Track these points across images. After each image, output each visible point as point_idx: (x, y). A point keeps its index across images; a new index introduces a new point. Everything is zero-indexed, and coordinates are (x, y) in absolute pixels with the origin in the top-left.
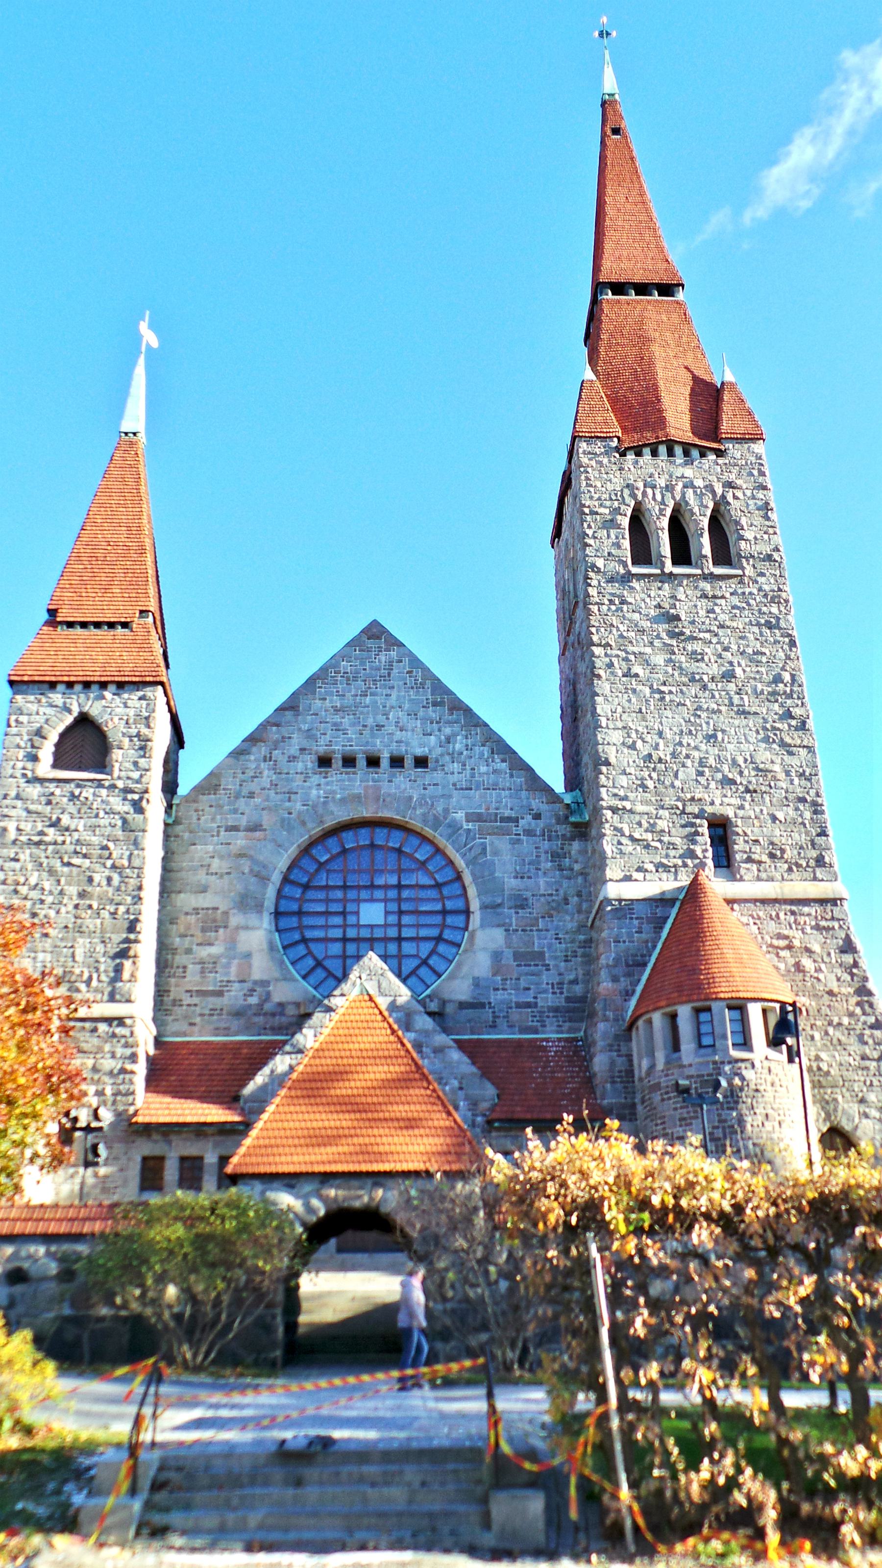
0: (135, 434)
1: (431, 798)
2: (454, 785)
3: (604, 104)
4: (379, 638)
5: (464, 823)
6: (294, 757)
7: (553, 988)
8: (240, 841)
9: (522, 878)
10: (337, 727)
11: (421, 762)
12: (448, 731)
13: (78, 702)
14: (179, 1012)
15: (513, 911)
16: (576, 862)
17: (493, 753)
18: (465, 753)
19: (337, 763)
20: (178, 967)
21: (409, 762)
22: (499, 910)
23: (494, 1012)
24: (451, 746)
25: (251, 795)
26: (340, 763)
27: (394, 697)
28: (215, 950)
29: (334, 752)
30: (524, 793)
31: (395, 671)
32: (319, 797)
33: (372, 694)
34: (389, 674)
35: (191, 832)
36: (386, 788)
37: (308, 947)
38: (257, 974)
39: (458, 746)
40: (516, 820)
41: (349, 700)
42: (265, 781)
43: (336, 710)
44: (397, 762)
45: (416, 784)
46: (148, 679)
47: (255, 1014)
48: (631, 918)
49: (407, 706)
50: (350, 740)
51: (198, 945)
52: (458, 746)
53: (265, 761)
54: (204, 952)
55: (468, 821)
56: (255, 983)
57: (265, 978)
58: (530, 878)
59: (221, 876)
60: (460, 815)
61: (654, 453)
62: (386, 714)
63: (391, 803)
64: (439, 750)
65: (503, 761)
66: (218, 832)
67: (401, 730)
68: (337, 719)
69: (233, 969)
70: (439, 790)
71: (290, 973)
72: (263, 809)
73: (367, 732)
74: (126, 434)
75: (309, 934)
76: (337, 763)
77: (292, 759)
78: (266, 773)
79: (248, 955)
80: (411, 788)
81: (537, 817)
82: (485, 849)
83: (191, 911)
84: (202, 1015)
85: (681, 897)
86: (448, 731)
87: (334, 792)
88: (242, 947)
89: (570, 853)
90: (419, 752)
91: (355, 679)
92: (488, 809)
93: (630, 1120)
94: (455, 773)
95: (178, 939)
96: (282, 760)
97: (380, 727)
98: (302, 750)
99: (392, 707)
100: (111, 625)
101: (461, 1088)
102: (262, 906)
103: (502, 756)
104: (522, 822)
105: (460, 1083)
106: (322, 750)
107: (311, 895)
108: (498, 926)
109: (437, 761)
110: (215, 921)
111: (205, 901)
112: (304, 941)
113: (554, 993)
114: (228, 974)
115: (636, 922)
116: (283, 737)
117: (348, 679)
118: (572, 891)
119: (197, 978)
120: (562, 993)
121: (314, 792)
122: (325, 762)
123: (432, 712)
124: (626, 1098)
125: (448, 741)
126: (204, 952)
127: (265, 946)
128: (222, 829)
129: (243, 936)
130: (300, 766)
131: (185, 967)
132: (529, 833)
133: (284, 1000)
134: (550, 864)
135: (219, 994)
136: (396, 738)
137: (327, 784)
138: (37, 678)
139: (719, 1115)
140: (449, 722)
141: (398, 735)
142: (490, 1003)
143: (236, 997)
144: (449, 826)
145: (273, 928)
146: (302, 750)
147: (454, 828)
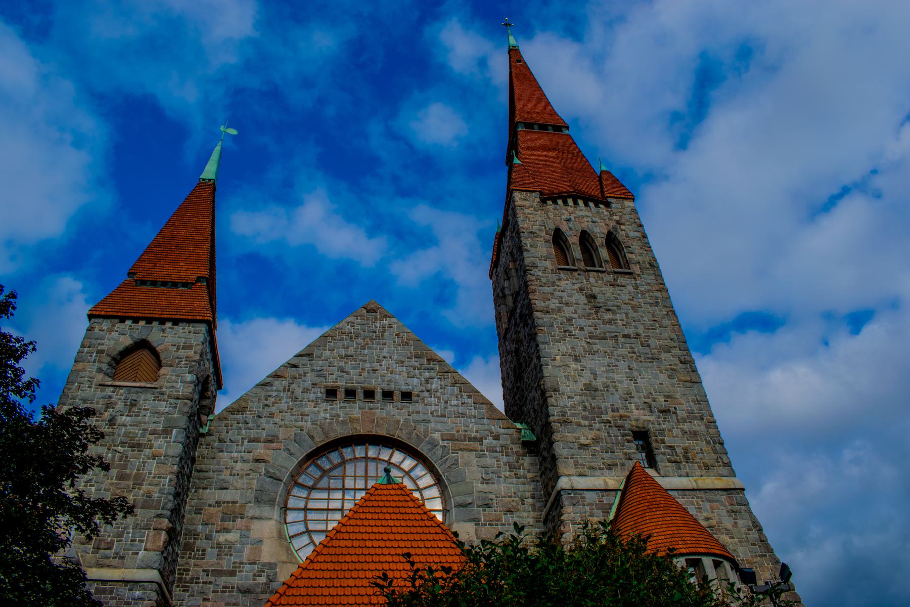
0: (210, 180)
1: (415, 421)
2: (432, 413)
3: (510, 51)
4: (375, 311)
6: (308, 390)
8: (260, 450)
9: (487, 483)
10: (342, 370)
11: (407, 396)
12: (427, 375)
13: (140, 330)
14: (196, 588)
15: (481, 509)
16: (529, 472)
17: (461, 391)
18: (440, 390)
19: (341, 394)
20: (198, 550)
21: (397, 395)
22: (470, 508)
24: (429, 385)
25: (271, 415)
26: (343, 395)
27: (386, 350)
28: (232, 537)
29: (338, 387)
30: (485, 421)
31: (387, 333)
32: (326, 419)
33: (369, 348)
34: (382, 336)
35: (220, 441)
36: (379, 414)
37: (311, 538)
38: (266, 557)
39: (434, 386)
40: (480, 440)
41: (351, 351)
42: (284, 407)
43: (342, 358)
44: (388, 395)
45: (402, 411)
46: (198, 318)
47: (262, 592)
48: (584, 505)
49: (395, 357)
50: (352, 379)
51: (217, 532)
52: (434, 386)
53: (284, 391)
54: (222, 538)
56: (264, 565)
57: (273, 561)
58: (493, 483)
59: (242, 477)
60: (437, 436)
61: (565, 203)
62: (379, 361)
63: (383, 425)
64: (420, 388)
65: (469, 397)
67: (391, 373)
68: (342, 364)
70: (420, 417)
71: (295, 557)
72: (280, 427)
73: (365, 375)
74: (204, 180)
75: (311, 527)
76: (341, 394)
77: (306, 390)
78: (284, 400)
79: (260, 541)
80: (399, 414)
81: (497, 438)
82: (457, 460)
83: (213, 503)
84: (215, 592)
85: (621, 488)
86: (427, 375)
87: (338, 415)
88: (254, 534)
89: (523, 466)
90: (404, 388)
91: (357, 337)
92: (458, 431)
95: (200, 527)
96: (298, 392)
97: (375, 370)
98: (314, 384)
99: (384, 357)
100: (175, 285)
102: (274, 501)
103: (468, 394)
104: (485, 442)
106: (330, 384)
107: (315, 495)
108: (470, 520)
109: (418, 396)
110: (234, 512)
111: (226, 495)
112: (308, 532)
115: (587, 508)
116: (300, 375)
117: (351, 338)
118: (528, 494)
119: (214, 560)
121: (322, 414)
123: (413, 362)
125: (427, 381)
126: (222, 538)
127: (275, 535)
129: (256, 525)
130: (312, 396)
131: (204, 550)
132: (492, 450)
134: (508, 473)
135: (232, 573)
136: (386, 379)
137: (332, 409)
138: (111, 313)
140: (428, 369)
141: (389, 377)
143: (246, 577)
144: (429, 443)
145: (283, 521)
146: (314, 384)
147: (433, 444)
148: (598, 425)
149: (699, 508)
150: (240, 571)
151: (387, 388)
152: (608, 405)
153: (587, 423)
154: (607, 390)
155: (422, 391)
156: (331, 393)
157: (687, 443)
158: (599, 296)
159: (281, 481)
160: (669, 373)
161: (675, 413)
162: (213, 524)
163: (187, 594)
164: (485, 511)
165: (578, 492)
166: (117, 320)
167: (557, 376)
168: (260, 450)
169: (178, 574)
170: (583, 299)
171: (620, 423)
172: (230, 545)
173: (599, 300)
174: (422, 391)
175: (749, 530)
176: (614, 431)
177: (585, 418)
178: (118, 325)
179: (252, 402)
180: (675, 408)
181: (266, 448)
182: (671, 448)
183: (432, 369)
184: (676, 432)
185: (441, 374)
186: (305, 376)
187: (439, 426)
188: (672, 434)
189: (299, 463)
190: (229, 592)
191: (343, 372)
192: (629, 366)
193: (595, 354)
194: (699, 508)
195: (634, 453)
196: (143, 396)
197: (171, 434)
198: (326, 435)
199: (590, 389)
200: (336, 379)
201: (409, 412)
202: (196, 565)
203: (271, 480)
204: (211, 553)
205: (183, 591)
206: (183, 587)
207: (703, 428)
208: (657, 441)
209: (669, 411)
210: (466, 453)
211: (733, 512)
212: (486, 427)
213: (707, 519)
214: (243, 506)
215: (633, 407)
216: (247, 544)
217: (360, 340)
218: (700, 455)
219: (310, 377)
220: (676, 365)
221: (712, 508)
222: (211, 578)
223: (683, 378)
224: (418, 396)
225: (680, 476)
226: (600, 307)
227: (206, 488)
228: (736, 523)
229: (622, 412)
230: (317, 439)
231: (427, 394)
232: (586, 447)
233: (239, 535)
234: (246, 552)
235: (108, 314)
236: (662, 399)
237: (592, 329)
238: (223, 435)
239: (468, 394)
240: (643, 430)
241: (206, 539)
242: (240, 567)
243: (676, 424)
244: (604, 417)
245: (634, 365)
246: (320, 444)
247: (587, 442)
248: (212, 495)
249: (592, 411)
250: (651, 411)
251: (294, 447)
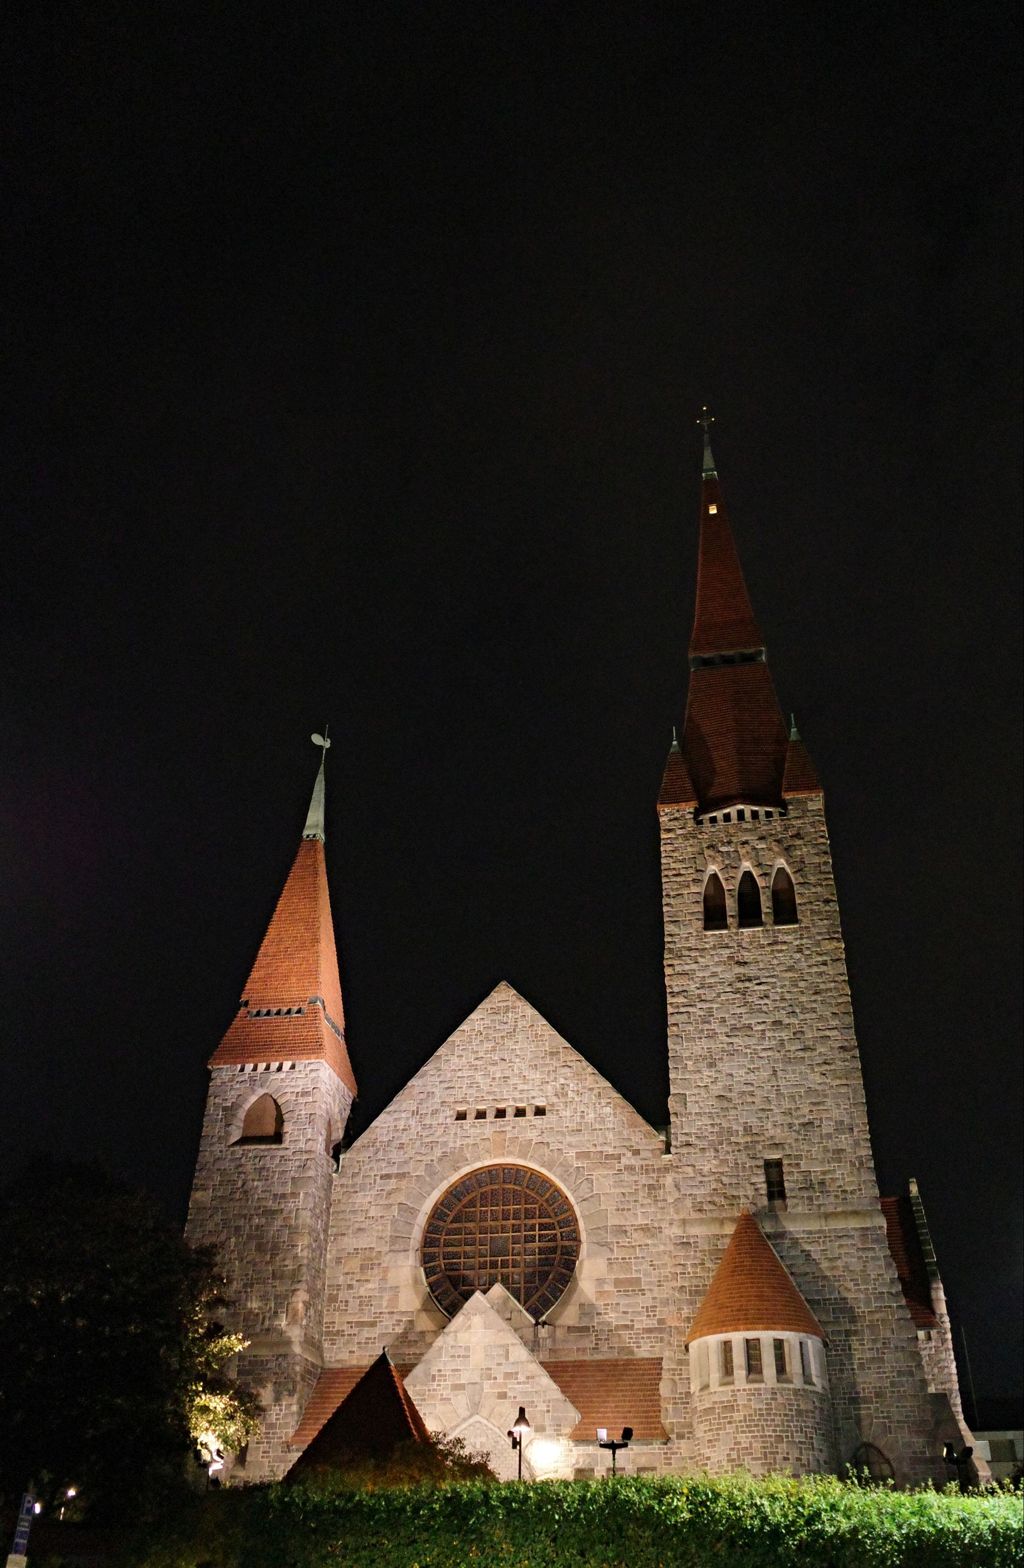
7: (647, 1311)
40: (619, 1158)
55: (577, 1158)
66: (375, 1181)
69: (385, 1304)
81: (636, 1152)
88: (391, 1283)
93: (689, 1438)
94: (565, 1116)
101: (548, 1411)
104: (623, 1160)
105: (548, 1406)
111: (363, 1242)
113: (648, 1316)
114: (380, 1306)
120: (654, 1316)
124: (685, 1418)
128: (378, 1178)
131: (347, 1302)
133: (425, 1329)
135: (373, 1324)
139: (735, 1438)
144: (561, 1164)
147: (565, 1167)
149: (824, 1250)
150: (380, 1322)
163: (335, 1347)
169: (326, 1327)
176: (743, 1158)
188: (811, 1155)
190: (372, 1343)
193: (733, 1055)
204: (354, 1304)
205: (332, 1344)
206: (330, 1340)
222: (355, 1331)
248: (350, 1243)
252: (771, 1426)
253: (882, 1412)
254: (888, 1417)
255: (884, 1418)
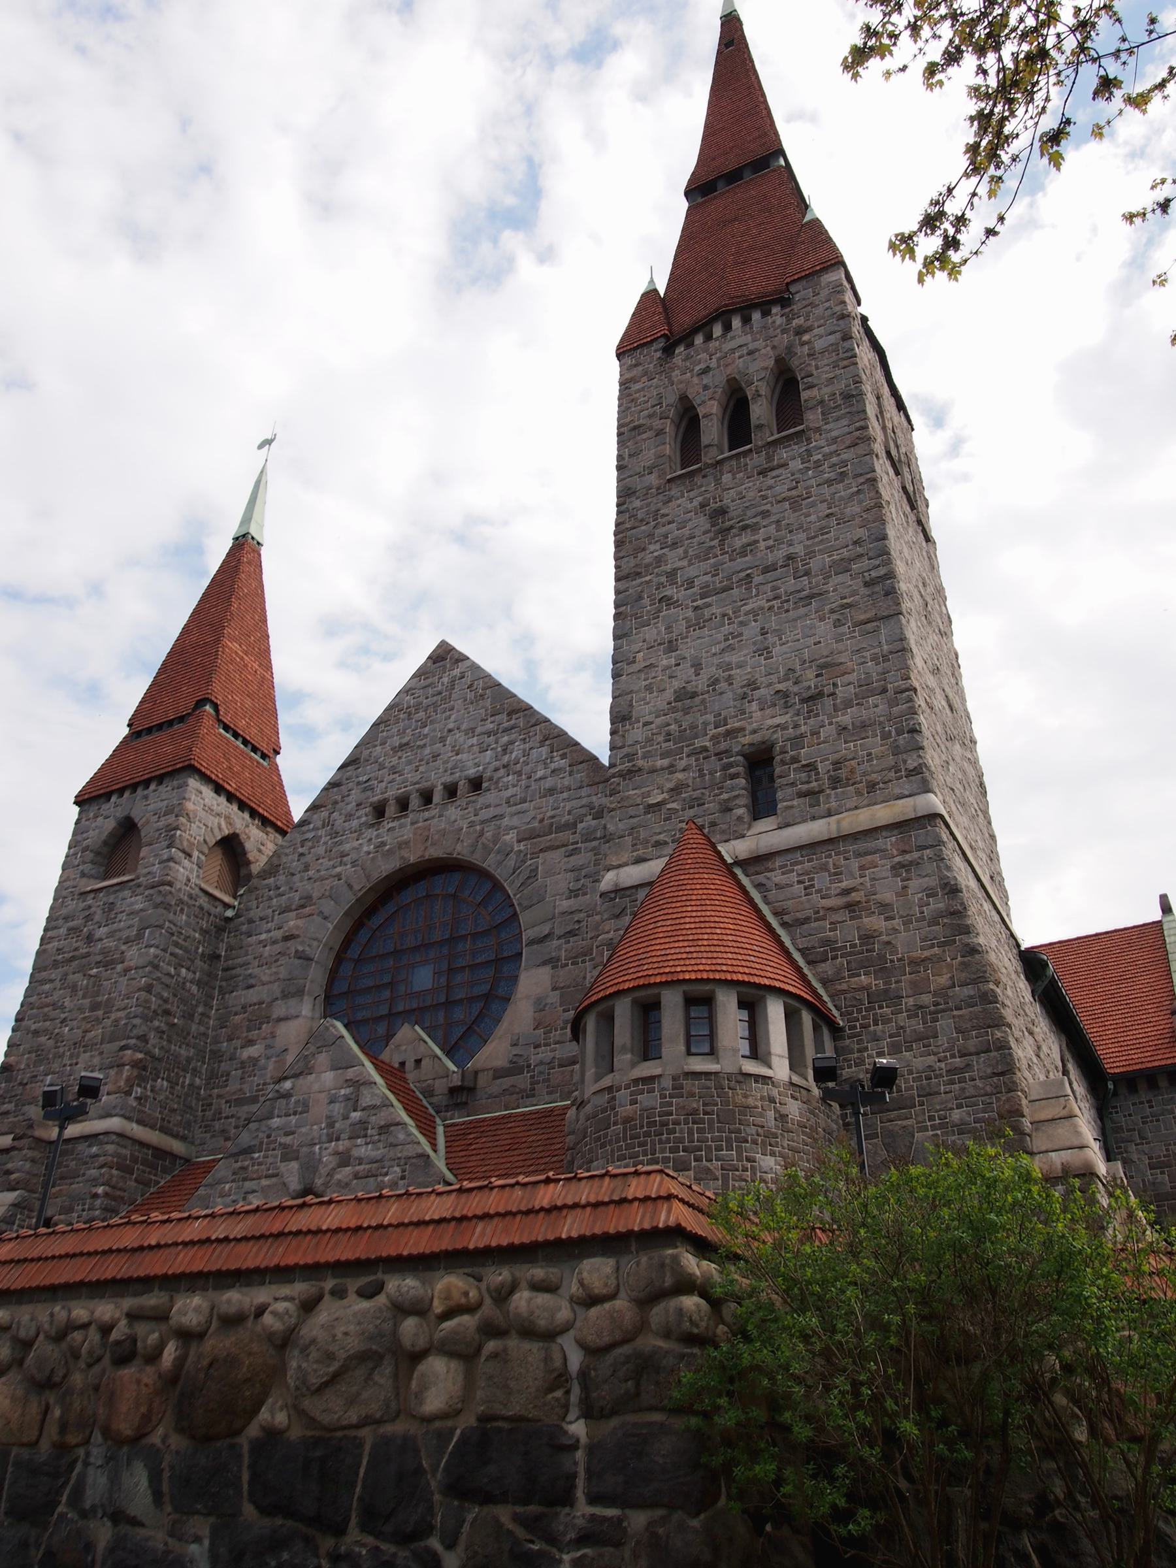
5: (516, 845)
11: (476, 784)
12: (505, 739)
20: (222, 1076)
23: (532, 1077)
28: (253, 1051)
36: (438, 824)
42: (321, 850)
54: (247, 1053)
65: (563, 756)
66: (273, 917)
72: (315, 882)
77: (349, 817)
82: (537, 868)
84: (236, 1127)
88: (279, 1043)
90: (472, 772)
105: (404, 1171)
108: (544, 963)
111: (252, 996)
122: (379, 811)
125: (505, 751)
126: (247, 1053)
130: (355, 823)
131: (228, 1074)
142: (529, 1066)
148: (683, 764)
149: (836, 874)
151: (448, 779)
152: (710, 718)
153: (665, 762)
154: (714, 690)
155: (496, 770)
156: (379, 811)
157: (846, 749)
158: (732, 506)
159: (312, 960)
160: (835, 616)
161: (833, 694)
162: (238, 1038)
164: (569, 942)
165: (628, 893)
166: (102, 800)
167: (631, 692)
168: (292, 923)
170: (703, 522)
171: (723, 746)
172: (254, 1061)
173: (732, 514)
174: (496, 770)
175: (928, 896)
177: (664, 755)
178: (105, 806)
179: (287, 855)
180: (834, 685)
181: (298, 917)
182: (811, 767)
183: (513, 728)
184: (828, 731)
185: (525, 731)
186: (348, 795)
187: (515, 821)
189: (335, 928)
191: (395, 773)
192: (762, 629)
194: (836, 874)
195: (737, 797)
196: (121, 895)
197: (143, 938)
198: (368, 877)
199: (684, 696)
200: (386, 788)
201: (475, 810)
202: (219, 1096)
203: (301, 961)
207: (882, 708)
208: (783, 763)
209: (820, 694)
210: (550, 855)
211: (904, 866)
212: (584, 801)
213: (846, 892)
214: (270, 1005)
215: (754, 706)
216: (271, 1057)
217: (422, 714)
218: (866, 766)
219: (355, 795)
220: (854, 593)
221: (862, 868)
223: (862, 617)
224: (491, 779)
225: (814, 818)
226: (732, 527)
227: (232, 992)
228: (905, 887)
229: (734, 724)
230: (357, 887)
231: (502, 772)
232: (656, 809)
233: (263, 1046)
234: (271, 1067)
235: (93, 794)
236: (811, 674)
237: (708, 578)
238: (252, 914)
239: (561, 752)
240: (763, 746)
241: (230, 1060)
242: (263, 1090)
243: (830, 716)
244: (698, 743)
245: (773, 623)
246: (360, 894)
247: (659, 798)
249: (682, 736)
250: (787, 706)
251: (328, 906)
252: (668, 1141)
253: (931, 1118)
254: (941, 1126)
255: (934, 1128)
